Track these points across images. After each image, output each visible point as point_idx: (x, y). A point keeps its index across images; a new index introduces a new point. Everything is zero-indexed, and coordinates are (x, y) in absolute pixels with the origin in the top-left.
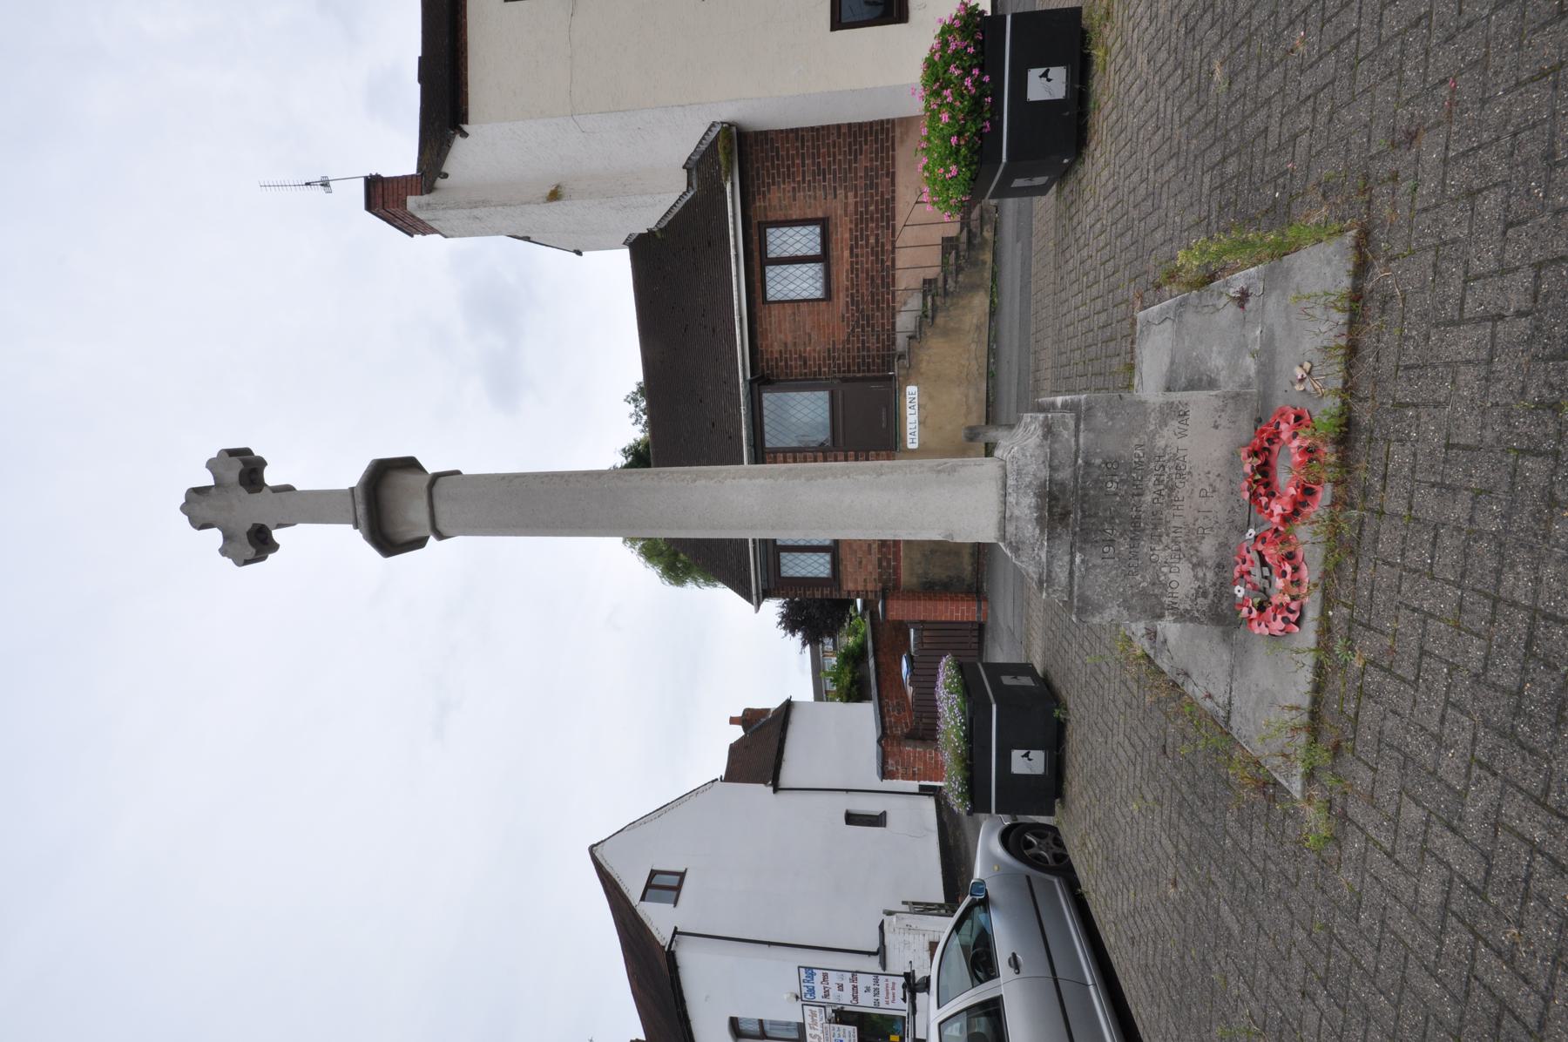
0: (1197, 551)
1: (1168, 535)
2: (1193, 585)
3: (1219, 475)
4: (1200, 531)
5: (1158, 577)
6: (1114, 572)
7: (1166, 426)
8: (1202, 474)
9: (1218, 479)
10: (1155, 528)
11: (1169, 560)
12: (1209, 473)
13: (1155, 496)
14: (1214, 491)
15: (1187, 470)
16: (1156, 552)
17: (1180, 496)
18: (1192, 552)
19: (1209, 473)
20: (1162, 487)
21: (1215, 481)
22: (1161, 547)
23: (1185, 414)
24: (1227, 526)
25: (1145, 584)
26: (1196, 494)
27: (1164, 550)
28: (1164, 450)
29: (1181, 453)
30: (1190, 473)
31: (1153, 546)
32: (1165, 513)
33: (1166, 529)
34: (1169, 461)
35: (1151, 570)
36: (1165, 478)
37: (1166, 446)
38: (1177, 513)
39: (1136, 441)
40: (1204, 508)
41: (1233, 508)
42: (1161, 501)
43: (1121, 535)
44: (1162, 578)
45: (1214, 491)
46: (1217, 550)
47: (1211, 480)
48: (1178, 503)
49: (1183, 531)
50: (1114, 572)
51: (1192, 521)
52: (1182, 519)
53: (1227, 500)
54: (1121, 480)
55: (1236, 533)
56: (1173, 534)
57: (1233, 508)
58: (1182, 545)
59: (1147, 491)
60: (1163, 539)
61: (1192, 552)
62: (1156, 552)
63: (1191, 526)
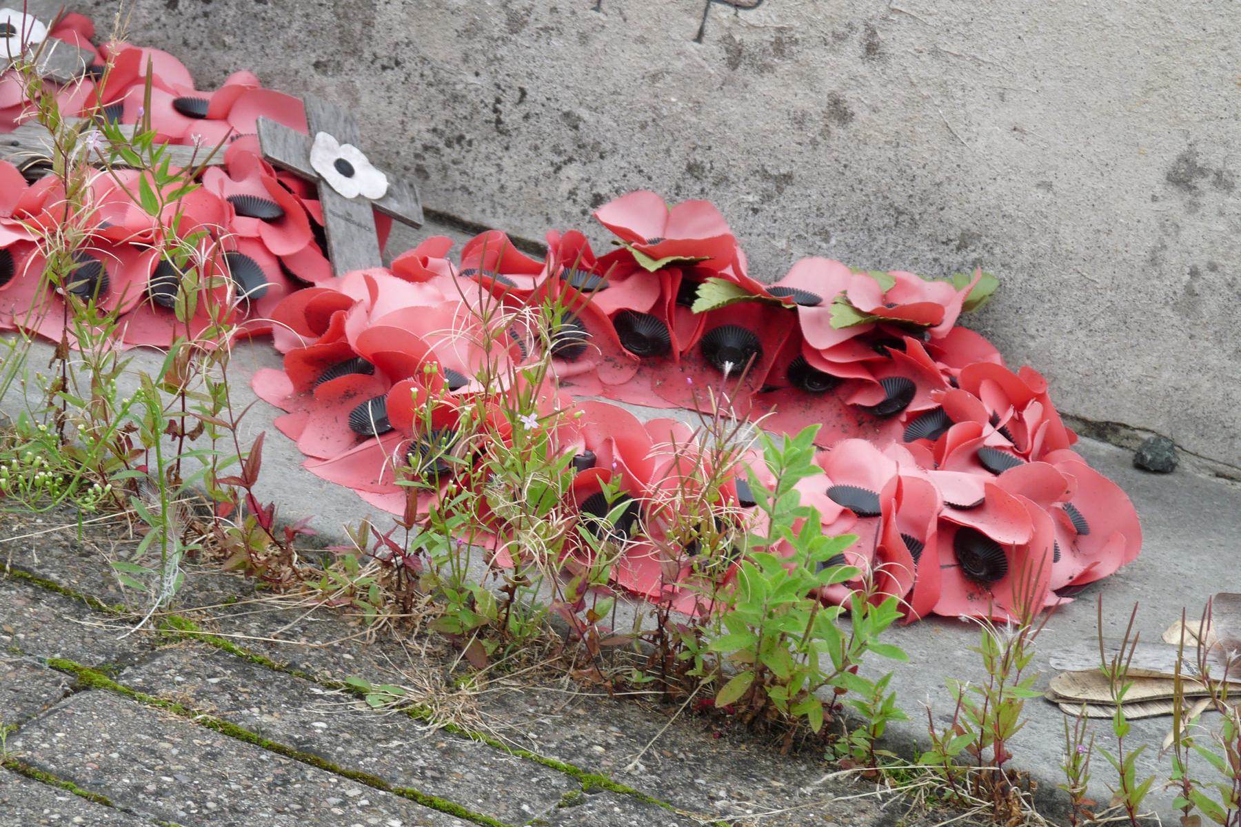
3: (839, 111)
9: (812, 104)
12: (872, 49)
14: (735, 56)
19: (872, 49)
21: (810, 79)
41: (591, 151)
45: (735, 56)
47: (815, 55)
55: (420, 129)
57: (591, 151)
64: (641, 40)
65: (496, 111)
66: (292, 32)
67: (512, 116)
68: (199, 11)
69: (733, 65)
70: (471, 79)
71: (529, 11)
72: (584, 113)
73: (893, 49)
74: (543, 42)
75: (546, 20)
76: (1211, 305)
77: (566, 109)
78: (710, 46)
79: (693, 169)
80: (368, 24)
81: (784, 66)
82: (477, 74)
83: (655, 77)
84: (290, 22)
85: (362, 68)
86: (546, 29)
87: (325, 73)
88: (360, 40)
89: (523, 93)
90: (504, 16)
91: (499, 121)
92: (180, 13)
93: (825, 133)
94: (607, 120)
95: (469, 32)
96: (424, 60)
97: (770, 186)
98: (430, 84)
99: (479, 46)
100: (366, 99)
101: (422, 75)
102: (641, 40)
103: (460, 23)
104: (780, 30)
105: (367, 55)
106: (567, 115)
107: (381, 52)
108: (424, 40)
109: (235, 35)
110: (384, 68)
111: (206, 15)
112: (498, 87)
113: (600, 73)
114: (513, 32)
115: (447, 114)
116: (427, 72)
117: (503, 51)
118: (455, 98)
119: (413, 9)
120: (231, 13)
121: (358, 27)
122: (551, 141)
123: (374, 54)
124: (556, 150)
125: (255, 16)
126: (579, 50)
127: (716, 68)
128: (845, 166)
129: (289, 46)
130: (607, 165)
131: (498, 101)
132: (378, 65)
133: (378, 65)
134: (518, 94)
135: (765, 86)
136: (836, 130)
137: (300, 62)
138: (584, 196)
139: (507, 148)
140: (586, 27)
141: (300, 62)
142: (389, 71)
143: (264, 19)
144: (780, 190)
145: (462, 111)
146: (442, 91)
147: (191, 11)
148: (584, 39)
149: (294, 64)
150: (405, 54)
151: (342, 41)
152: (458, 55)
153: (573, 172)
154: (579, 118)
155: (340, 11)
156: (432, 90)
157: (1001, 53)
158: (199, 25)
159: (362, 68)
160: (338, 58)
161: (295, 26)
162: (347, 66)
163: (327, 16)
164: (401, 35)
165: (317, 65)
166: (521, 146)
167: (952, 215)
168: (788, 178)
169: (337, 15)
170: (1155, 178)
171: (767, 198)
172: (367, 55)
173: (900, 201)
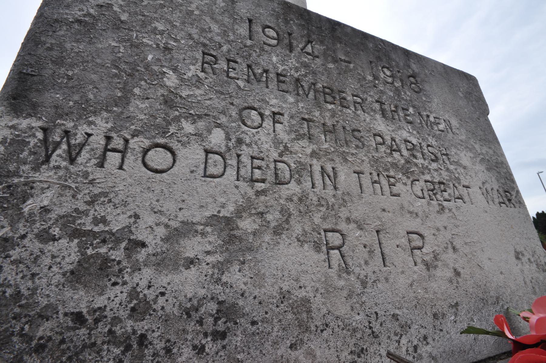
0: (277, 231)
1: (314, 154)
2: (149, 219)
3: (457, 274)
4: (335, 239)
5: (195, 118)
6: (215, 28)
7: (489, 169)
8: (448, 236)
9: (449, 274)
10: (327, 130)
11: (245, 151)
12: (454, 248)
13: (388, 138)
15: (445, 204)
16: (268, 123)
17: (398, 188)
18: (273, 217)
19: (454, 248)
20: (405, 153)
22: (284, 136)
23: (509, 200)
24: (359, 318)
25: (171, 80)
26: (414, 225)
27: (277, 142)
28: (457, 163)
29: (464, 192)
30: (442, 209)
31: (285, 119)
32: (362, 155)
33: (327, 153)
34: (448, 169)
35: (218, 103)
36: (420, 161)
37: (465, 168)
38: (366, 181)
39: (454, 122)
40: (389, 246)
42: (382, 149)
43: (306, 66)
44: (188, 127)
45: (428, 266)
46: (284, 296)
48: (384, 182)
49: (330, 191)
50: (215, 28)
51: (355, 215)
52: (356, 190)
53: (418, 304)
54: (397, 89)
56: (317, 168)
58: (293, 188)
59: (393, 127)
60: (304, 143)
61: (273, 217)
62: (268, 123)
63: (344, 213)
64: (403, 272)
65: (371, 328)
66: (274, 334)
67: (377, 328)
68: (219, 346)
69: (428, 269)
70: (358, 317)
71: (366, 277)
72: (397, 312)
73: (458, 246)
74: (375, 287)
75: (373, 278)
76: (537, 290)
77: (392, 313)
78: (421, 266)
79: (435, 316)
80: (309, 311)
81: (440, 264)
82: (359, 314)
83: (411, 285)
84: (272, 329)
85: (312, 337)
86: (375, 282)
87: (296, 349)
88: (308, 322)
89: (376, 313)
90: (359, 283)
91: (373, 332)
92: (208, 354)
93: (458, 282)
94: (405, 310)
95: (349, 296)
96: (337, 318)
97: (454, 310)
98: (343, 329)
99: (355, 301)
100: (318, 353)
101: (338, 326)
102: (403, 272)
103: (345, 293)
104: (433, 252)
105: (313, 328)
106: (393, 315)
107: (319, 324)
108: (334, 308)
109: (244, 352)
110: (322, 331)
111: (224, 347)
112: (367, 315)
113: (397, 291)
114: (365, 288)
115: (354, 341)
116: (340, 323)
117: (364, 299)
118: (355, 330)
119: (326, 295)
120: (239, 339)
121: (305, 315)
122: (392, 331)
123: (316, 326)
124: (396, 334)
125: (253, 334)
126: (387, 285)
127: (425, 273)
128: (466, 291)
129: (275, 343)
130: (412, 330)
131: (370, 323)
132: (319, 331)
133: (319, 331)
134: (375, 315)
135: (438, 273)
136: (460, 280)
137: (283, 350)
138: (411, 350)
139: (380, 344)
140: (385, 274)
141: (283, 350)
142: (325, 332)
143: (258, 334)
144: (457, 309)
145: (359, 336)
146: (349, 330)
147: (214, 349)
148: (387, 280)
149: (279, 353)
150: (330, 318)
151: (300, 326)
152: (349, 308)
153: (404, 341)
154: (397, 315)
155: (295, 310)
156: (345, 331)
157: (476, 238)
158: (221, 356)
159: (312, 337)
160: (300, 337)
161: (275, 329)
162: (306, 339)
163: (290, 316)
164: (324, 311)
165: (291, 347)
166: (383, 338)
167: (492, 293)
168: (457, 303)
169: (294, 313)
170: (514, 258)
171: (456, 315)
172: (313, 328)
173: (481, 295)
